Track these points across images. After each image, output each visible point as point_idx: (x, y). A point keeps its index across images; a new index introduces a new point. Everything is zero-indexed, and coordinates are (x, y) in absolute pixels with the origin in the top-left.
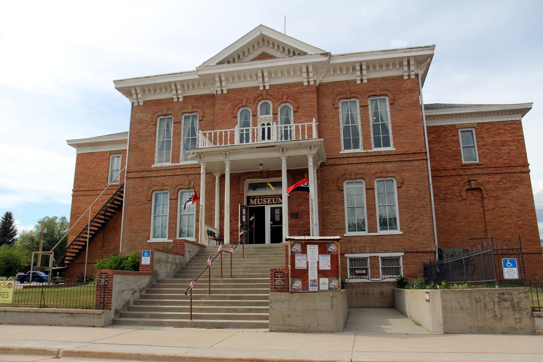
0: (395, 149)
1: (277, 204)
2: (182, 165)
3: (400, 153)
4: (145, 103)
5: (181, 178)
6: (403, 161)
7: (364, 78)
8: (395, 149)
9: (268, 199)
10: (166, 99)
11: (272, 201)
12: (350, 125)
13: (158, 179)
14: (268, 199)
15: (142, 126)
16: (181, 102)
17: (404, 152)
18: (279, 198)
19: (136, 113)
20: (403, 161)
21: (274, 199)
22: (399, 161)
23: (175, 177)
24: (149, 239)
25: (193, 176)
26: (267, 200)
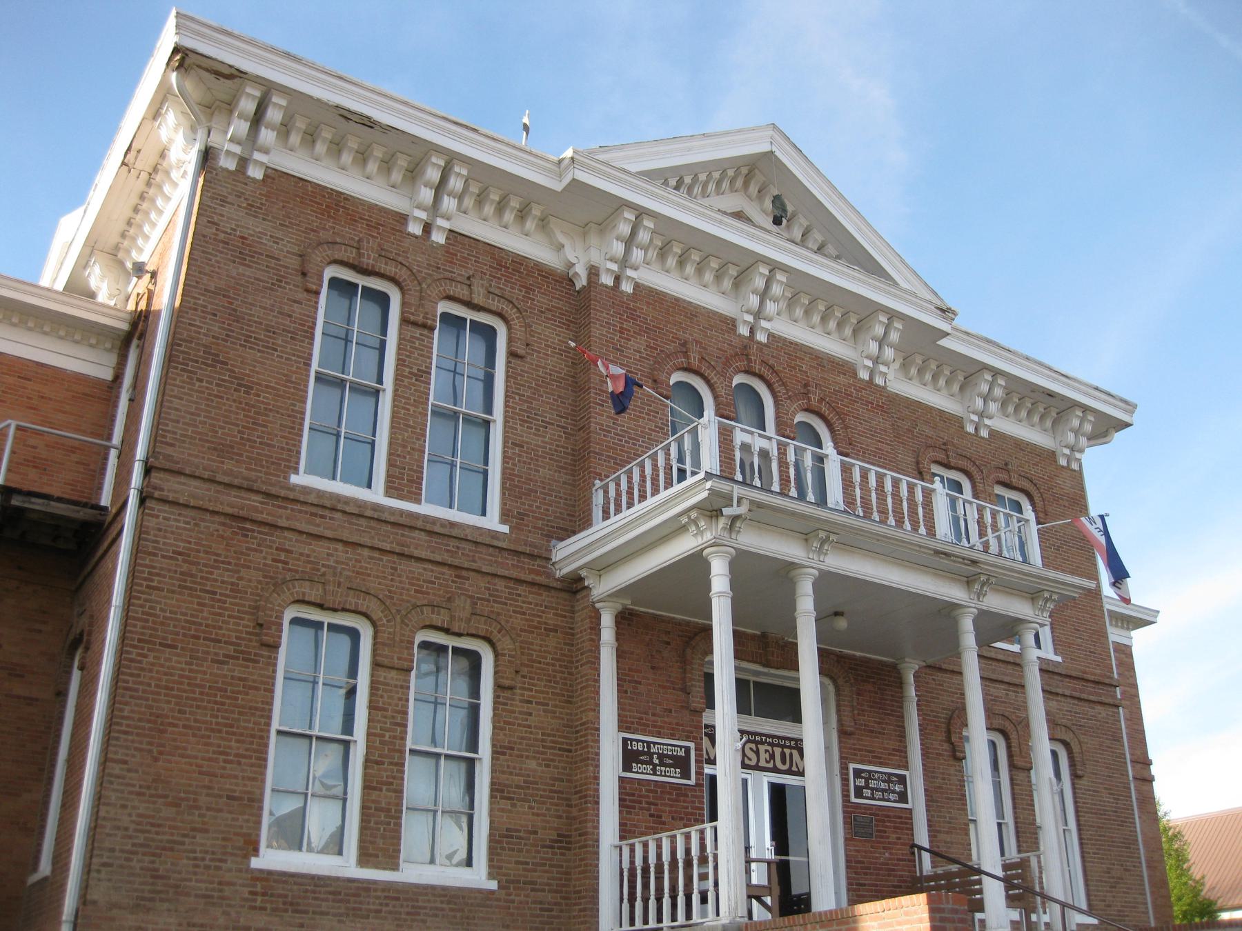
0: (505, 529)
1: (789, 772)
2: (426, 518)
3: (1074, 673)
4: (274, 176)
5: (428, 575)
6: (1079, 699)
7: (440, 222)
8: (505, 529)
9: (762, 748)
10: (373, 207)
11: (772, 756)
12: (350, 377)
13: (321, 548)
14: (762, 748)
15: (248, 272)
16: (436, 247)
17: (1080, 674)
18: (795, 753)
19: (224, 201)
20: (1079, 699)
21: (778, 751)
22: (1072, 697)
23: (404, 566)
24: (256, 852)
25: (482, 583)
26: (757, 753)
